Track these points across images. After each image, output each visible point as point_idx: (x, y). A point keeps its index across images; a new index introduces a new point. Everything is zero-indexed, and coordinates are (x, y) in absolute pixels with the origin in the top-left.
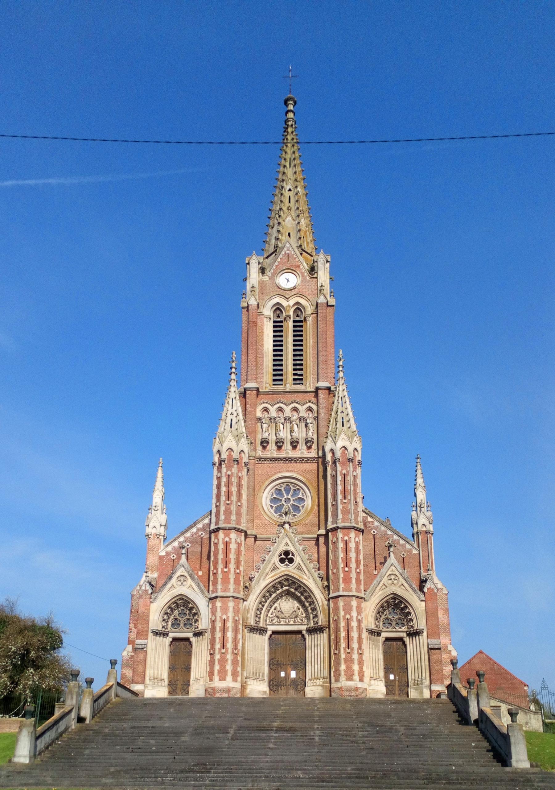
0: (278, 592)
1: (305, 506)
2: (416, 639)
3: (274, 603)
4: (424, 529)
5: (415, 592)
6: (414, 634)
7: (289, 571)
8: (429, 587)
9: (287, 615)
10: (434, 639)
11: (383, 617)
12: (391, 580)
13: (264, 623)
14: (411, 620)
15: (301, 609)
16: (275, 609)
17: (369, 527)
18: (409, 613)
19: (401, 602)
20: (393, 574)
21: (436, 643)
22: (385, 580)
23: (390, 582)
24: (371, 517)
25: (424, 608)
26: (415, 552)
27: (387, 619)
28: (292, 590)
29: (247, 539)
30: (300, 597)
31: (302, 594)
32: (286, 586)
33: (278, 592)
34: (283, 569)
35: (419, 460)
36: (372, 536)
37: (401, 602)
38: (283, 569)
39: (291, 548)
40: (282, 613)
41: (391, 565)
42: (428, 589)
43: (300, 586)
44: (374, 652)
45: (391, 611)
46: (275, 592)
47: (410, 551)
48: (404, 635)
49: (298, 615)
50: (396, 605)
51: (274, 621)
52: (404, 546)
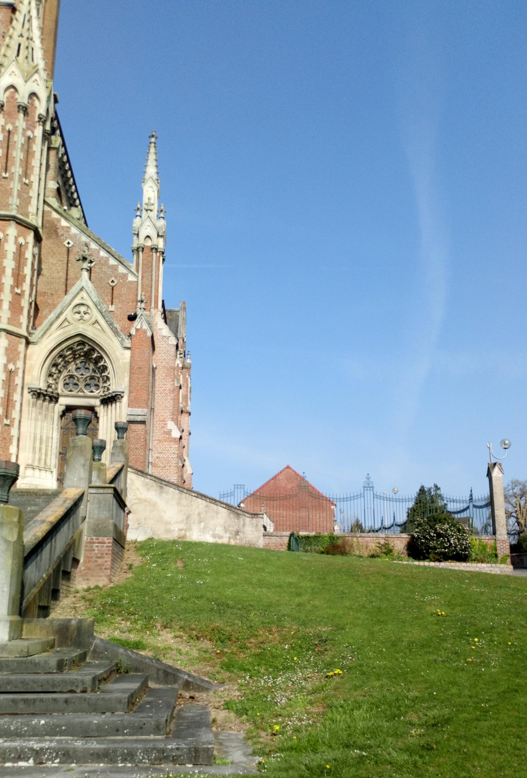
2: (112, 408)
4: (149, 243)
6: (109, 400)
8: (139, 327)
10: (139, 407)
11: (65, 373)
14: (108, 378)
17: (62, 235)
18: (105, 368)
19: (93, 350)
20: (83, 304)
21: (140, 413)
22: (68, 313)
24: (66, 219)
25: (128, 360)
26: (131, 278)
27: (72, 377)
35: (153, 140)
36: (65, 250)
37: (93, 350)
41: (82, 289)
42: (137, 330)
44: (39, 427)
45: (79, 365)
47: (125, 276)
48: (96, 402)
50: (83, 354)
52: (114, 268)
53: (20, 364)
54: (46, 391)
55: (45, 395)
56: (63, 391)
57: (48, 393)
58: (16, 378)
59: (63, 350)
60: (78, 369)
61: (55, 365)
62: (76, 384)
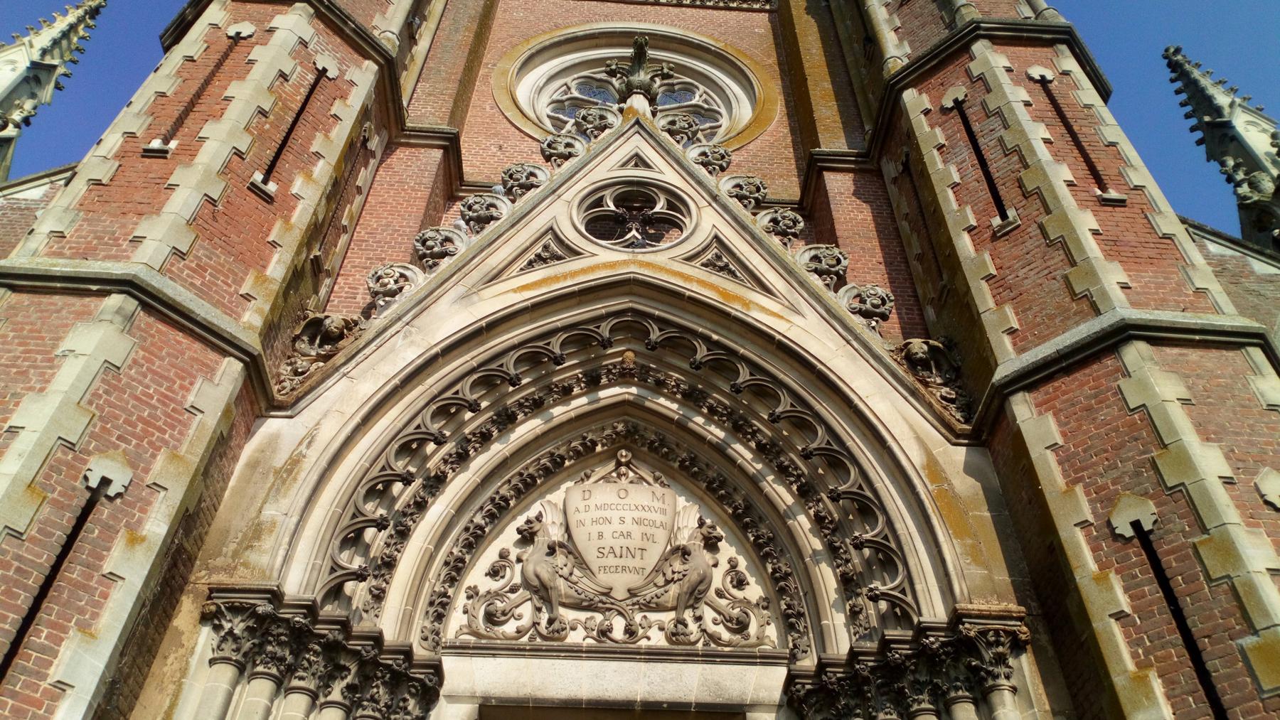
0: (560, 412)
1: (721, 131)
3: (527, 488)
7: (648, 265)
9: (620, 584)
13: (421, 622)
15: (727, 550)
16: (527, 537)
28: (668, 406)
29: (401, 154)
30: (719, 449)
31: (739, 428)
32: (624, 377)
33: (560, 412)
34: (606, 259)
38: (606, 259)
39: (667, 174)
40: (582, 563)
43: (724, 362)
46: (536, 406)
49: (704, 580)
51: (510, 628)
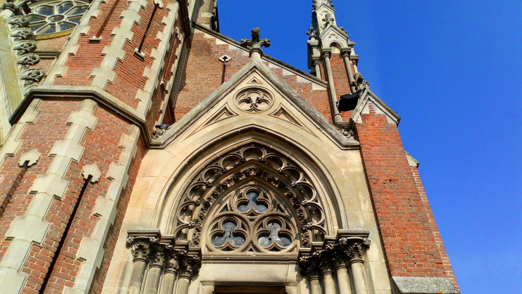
5: (321, 125)
8: (366, 111)
11: (216, 211)
12: (248, 101)
17: (217, 52)
18: (308, 190)
19: (277, 158)
23: (247, 106)
25: (359, 169)
27: (230, 219)
36: (220, 65)
37: (277, 158)
42: (364, 117)
48: (288, 272)
53: (118, 171)
54: (173, 241)
55: (168, 254)
56: (210, 250)
57: (177, 249)
58: (99, 201)
59: (218, 159)
60: (243, 203)
61: (197, 189)
62: (238, 234)
